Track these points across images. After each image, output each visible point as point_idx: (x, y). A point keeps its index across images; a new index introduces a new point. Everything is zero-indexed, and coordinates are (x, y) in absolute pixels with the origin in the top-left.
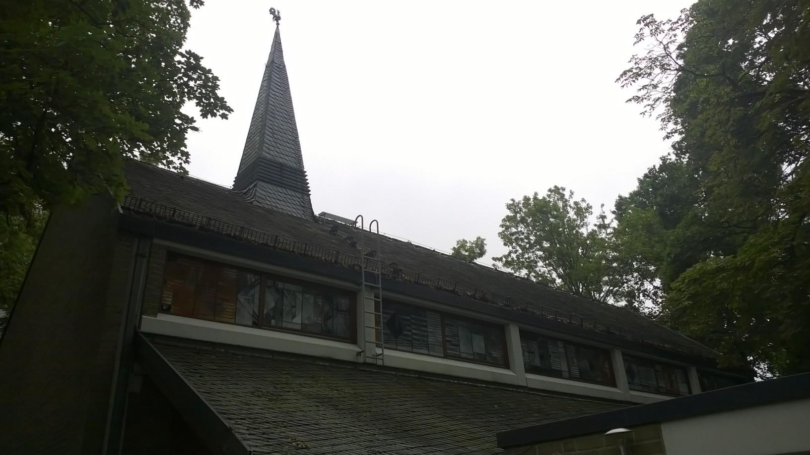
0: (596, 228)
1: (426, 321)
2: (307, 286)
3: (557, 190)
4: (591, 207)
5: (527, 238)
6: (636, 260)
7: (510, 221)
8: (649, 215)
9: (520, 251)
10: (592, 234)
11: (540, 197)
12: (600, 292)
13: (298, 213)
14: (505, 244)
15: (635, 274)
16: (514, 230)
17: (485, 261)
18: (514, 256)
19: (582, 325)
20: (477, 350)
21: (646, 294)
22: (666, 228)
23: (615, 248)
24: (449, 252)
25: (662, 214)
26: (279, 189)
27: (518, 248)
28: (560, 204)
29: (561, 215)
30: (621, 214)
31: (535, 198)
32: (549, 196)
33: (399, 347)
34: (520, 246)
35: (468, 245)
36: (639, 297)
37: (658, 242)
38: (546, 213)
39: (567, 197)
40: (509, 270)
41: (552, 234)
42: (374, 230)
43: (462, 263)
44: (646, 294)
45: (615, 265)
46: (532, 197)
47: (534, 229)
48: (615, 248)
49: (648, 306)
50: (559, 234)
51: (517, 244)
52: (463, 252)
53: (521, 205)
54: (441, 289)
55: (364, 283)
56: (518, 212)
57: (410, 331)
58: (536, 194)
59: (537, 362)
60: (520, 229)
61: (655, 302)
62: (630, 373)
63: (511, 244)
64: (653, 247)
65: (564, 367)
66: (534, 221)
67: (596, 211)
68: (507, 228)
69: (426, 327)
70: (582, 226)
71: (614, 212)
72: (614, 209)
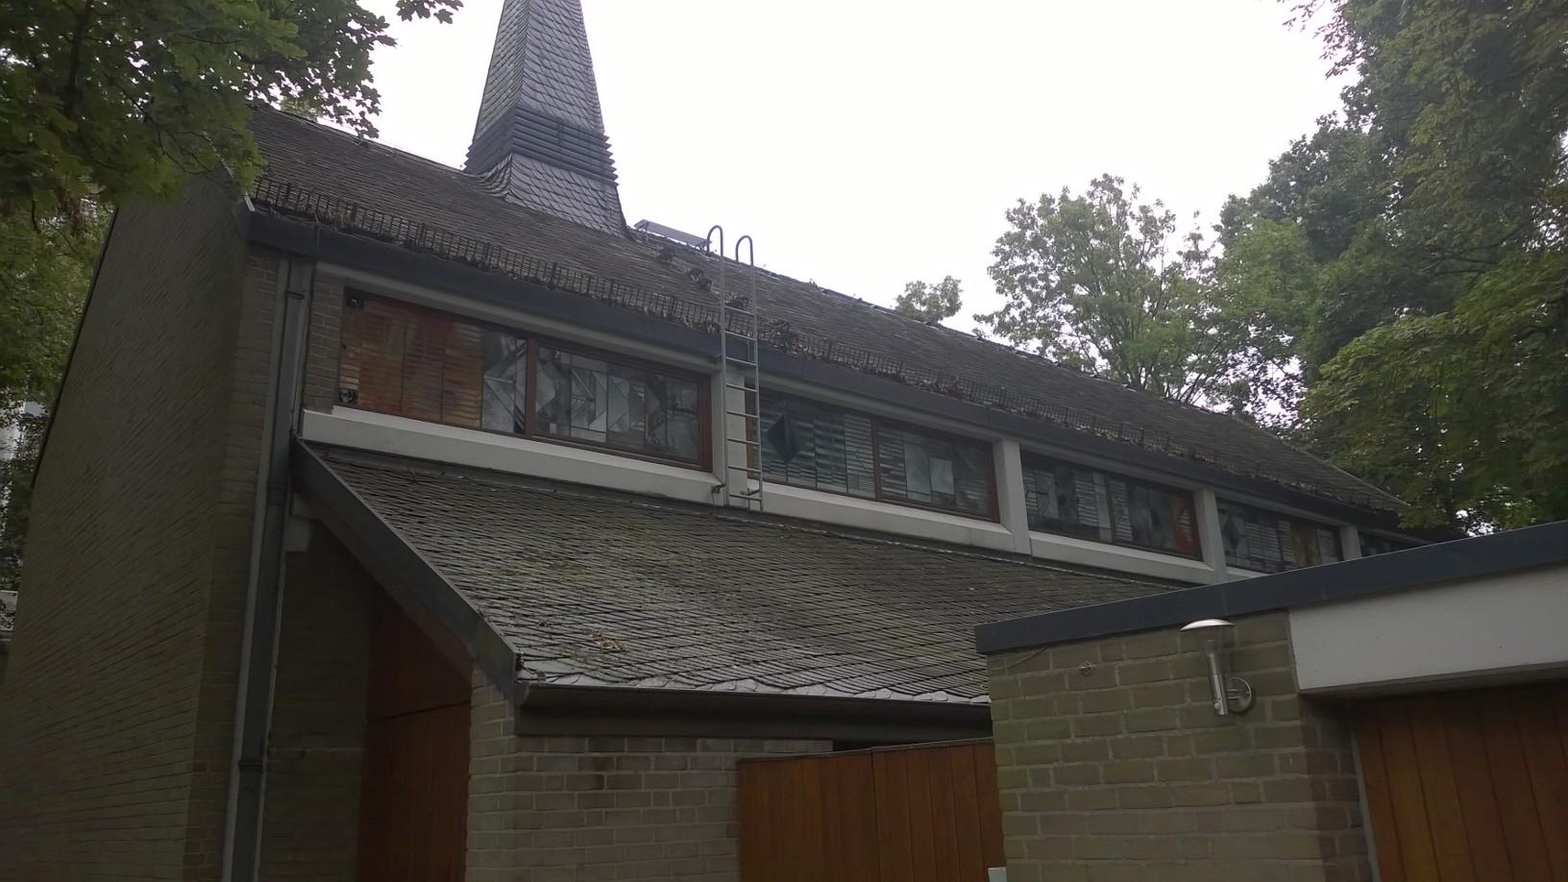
0: (1180, 260)
1: (843, 433)
2: (617, 362)
3: (1107, 183)
4: (1173, 217)
5: (1044, 277)
6: (1255, 322)
7: (1013, 244)
8: (1287, 234)
9: (1028, 304)
10: (1172, 272)
11: (1073, 197)
12: (1181, 383)
13: (595, 221)
14: (1000, 291)
15: (1252, 350)
16: (1018, 262)
17: (960, 323)
18: (1015, 313)
19: (1141, 445)
20: (939, 488)
21: (1269, 388)
22: (1320, 260)
23: (1216, 298)
24: (891, 304)
25: (1313, 234)
26: (557, 172)
27: (1025, 299)
28: (1113, 210)
29: (1113, 233)
30: (1232, 232)
31: (1064, 198)
32: (1091, 195)
33: (791, 480)
34: (1029, 293)
35: (927, 291)
36: (1255, 395)
37: (1299, 288)
38: (1082, 228)
39: (1126, 196)
40: (1005, 341)
41: (1094, 271)
42: (745, 259)
43: (913, 332)
44: (1269, 388)
45: (1213, 331)
46: (1057, 196)
47: (1058, 260)
48: (1216, 298)
49: (1272, 411)
50: (1108, 271)
51: (1024, 289)
52: (918, 307)
53: (1034, 213)
54: (873, 371)
55: (725, 357)
56: (1028, 227)
57: (812, 450)
58: (1065, 190)
59: (1053, 511)
60: (1030, 260)
61: (1286, 404)
62: (1230, 536)
63: (1012, 289)
64: (1289, 297)
65: (1104, 522)
66: (1059, 244)
67: (1184, 226)
68: (1006, 257)
69: (843, 442)
70: (1154, 255)
71: (1217, 228)
72: (1218, 221)
